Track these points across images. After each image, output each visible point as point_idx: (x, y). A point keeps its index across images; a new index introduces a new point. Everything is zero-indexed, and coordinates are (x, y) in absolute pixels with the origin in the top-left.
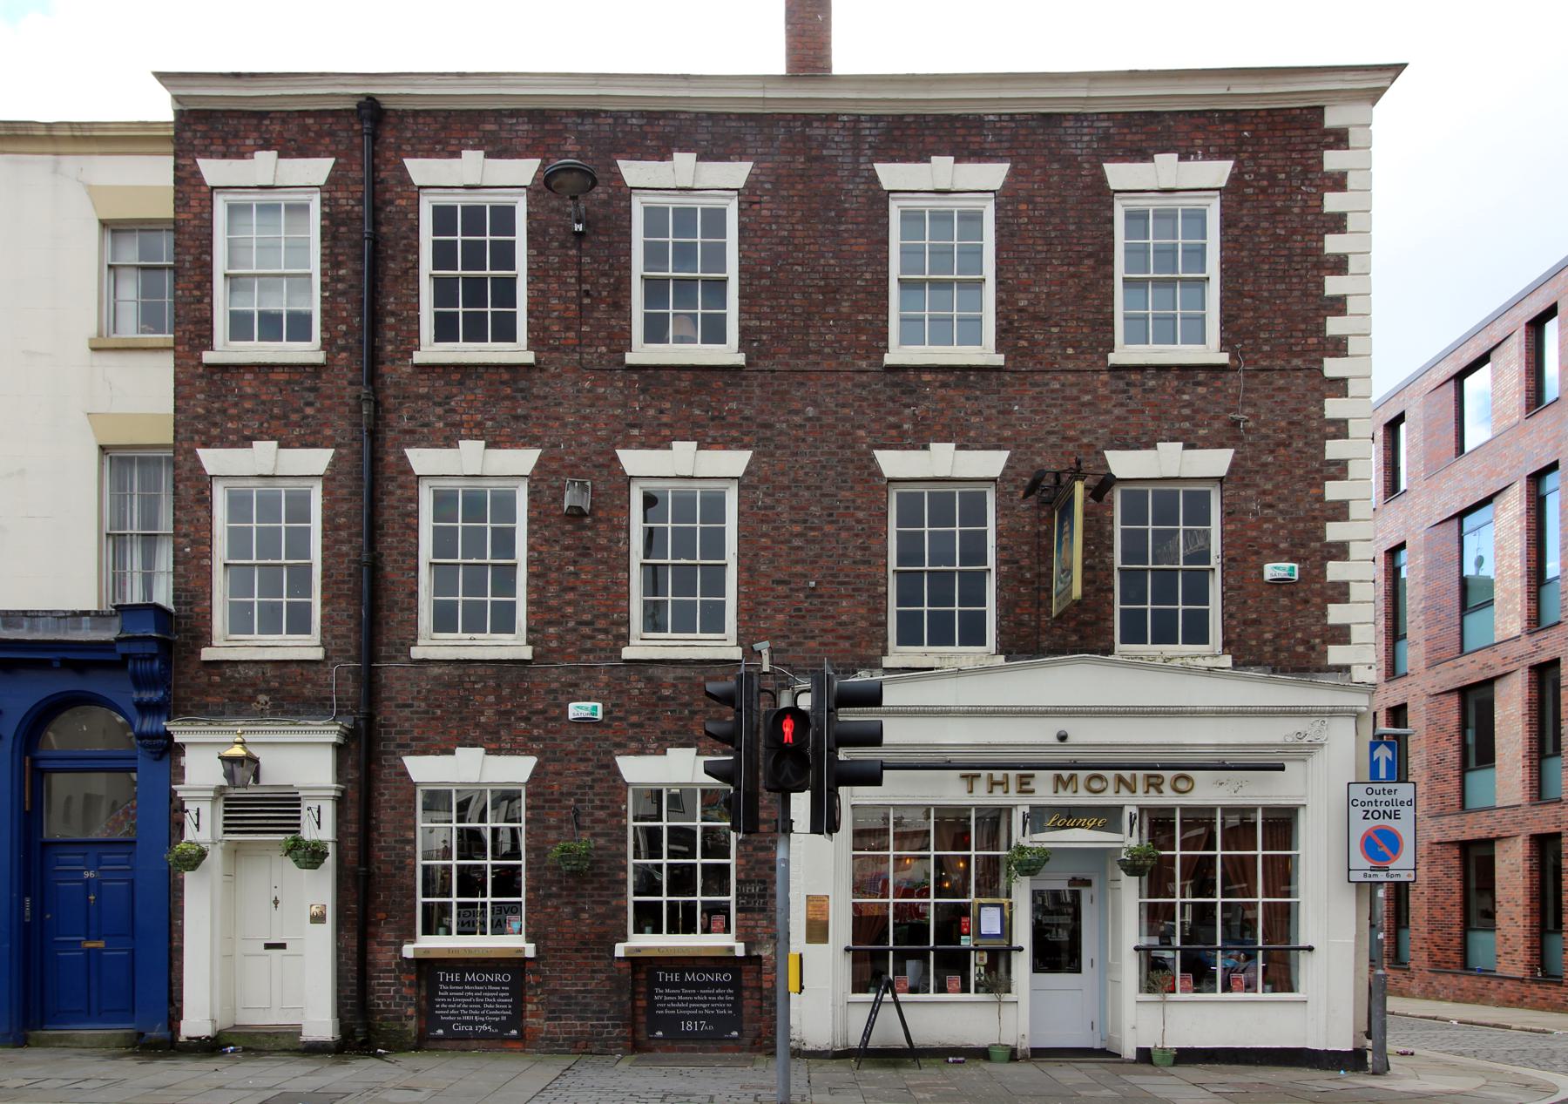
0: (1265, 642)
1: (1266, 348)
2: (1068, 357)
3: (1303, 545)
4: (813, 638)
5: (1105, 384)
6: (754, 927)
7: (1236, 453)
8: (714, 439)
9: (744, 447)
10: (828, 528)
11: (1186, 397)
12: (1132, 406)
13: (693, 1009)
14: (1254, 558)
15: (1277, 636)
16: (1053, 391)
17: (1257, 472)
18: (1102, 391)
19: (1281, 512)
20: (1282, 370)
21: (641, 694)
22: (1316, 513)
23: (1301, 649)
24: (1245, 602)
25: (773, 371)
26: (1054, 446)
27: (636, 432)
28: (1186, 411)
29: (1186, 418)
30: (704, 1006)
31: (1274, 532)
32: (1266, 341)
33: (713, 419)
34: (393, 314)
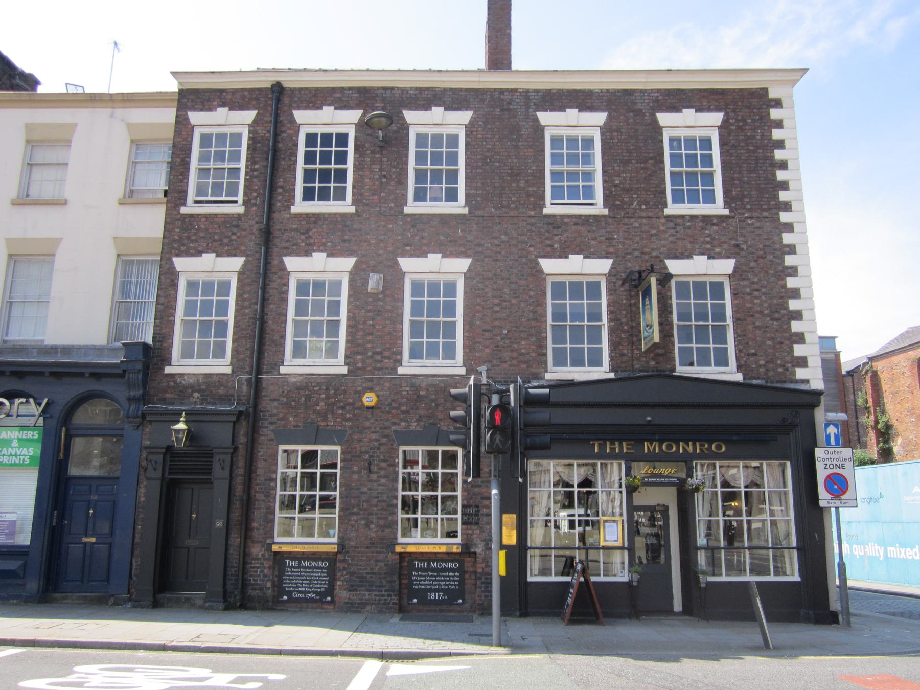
0: (760, 366)
1: (748, 207)
2: (642, 210)
3: (777, 312)
4: (506, 362)
5: (663, 225)
6: (471, 535)
7: (737, 261)
8: (451, 252)
9: (467, 256)
10: (514, 301)
11: (707, 232)
12: (678, 236)
13: (435, 585)
14: (751, 318)
15: (767, 362)
16: (635, 228)
17: (749, 272)
18: (662, 228)
19: (764, 294)
20: (758, 218)
21: (408, 394)
22: (783, 294)
23: (780, 370)
24: (748, 343)
25: (483, 216)
26: (637, 257)
27: (408, 248)
28: (708, 239)
29: (708, 243)
30: (442, 583)
31: (761, 305)
32: (748, 203)
33: (450, 241)
34: (281, 187)
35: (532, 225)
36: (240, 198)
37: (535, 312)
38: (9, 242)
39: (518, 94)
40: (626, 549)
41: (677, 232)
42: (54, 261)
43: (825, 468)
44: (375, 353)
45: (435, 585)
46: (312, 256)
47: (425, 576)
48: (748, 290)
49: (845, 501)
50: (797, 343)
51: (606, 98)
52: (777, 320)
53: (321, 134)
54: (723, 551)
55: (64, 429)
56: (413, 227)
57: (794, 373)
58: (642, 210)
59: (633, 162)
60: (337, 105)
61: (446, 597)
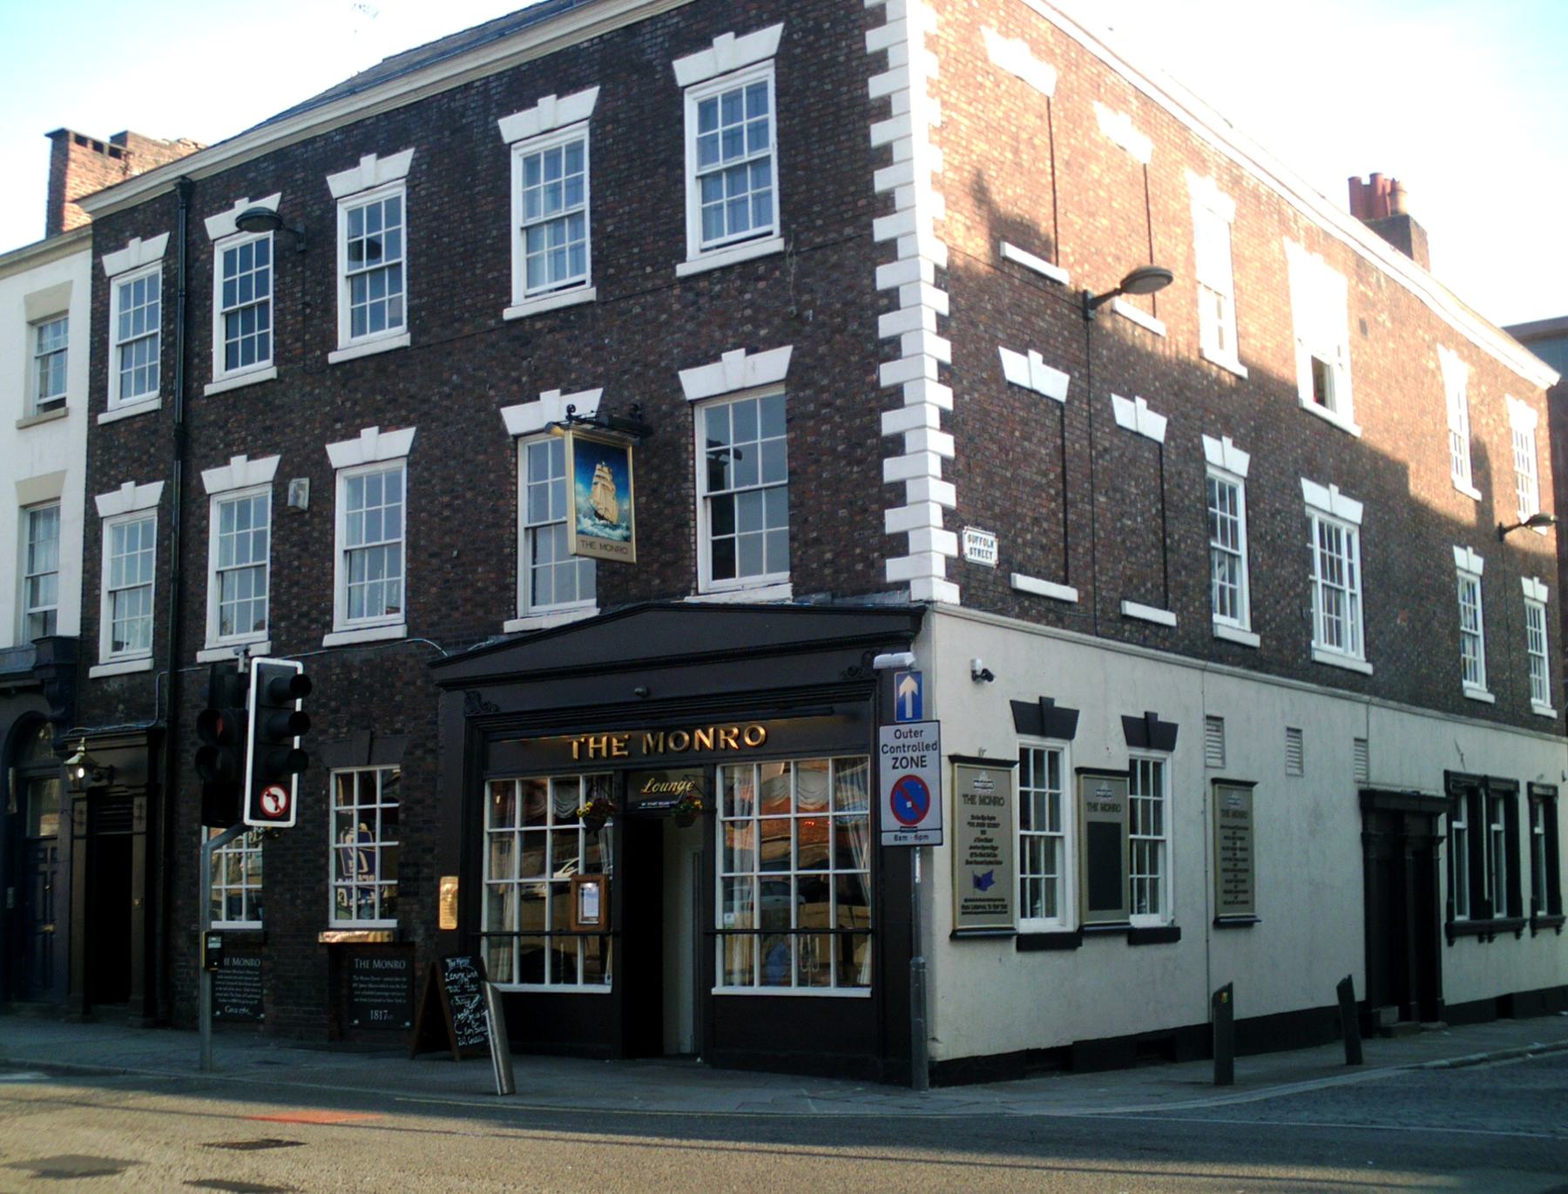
0: (825, 564)
1: (819, 222)
2: (646, 277)
3: (860, 445)
4: (457, 609)
5: (679, 298)
7: (794, 349)
8: (390, 421)
9: (409, 425)
10: (469, 495)
11: (748, 296)
12: (702, 316)
14: (813, 468)
15: (837, 555)
16: (637, 316)
17: (814, 368)
18: (676, 307)
19: (838, 410)
20: (835, 243)
21: (338, 679)
22: (873, 404)
23: (860, 567)
24: (806, 520)
25: (429, 346)
26: (639, 375)
27: (338, 426)
28: (748, 312)
29: (748, 320)
30: (387, 994)
31: (832, 434)
32: (819, 214)
33: (389, 402)
34: (198, 355)
35: (493, 346)
36: (775, 226)
37: (494, 511)
38: (20, 485)
39: (473, 92)
40: (720, 932)
41: (699, 309)
42: (58, 509)
43: (894, 767)
44: (301, 615)
45: (379, 997)
46: (538, 398)
47: (367, 982)
48: (812, 407)
49: (923, 833)
50: (892, 505)
51: (597, 56)
52: (860, 462)
53: (546, 153)
54: (547, 928)
55: (11, 771)
56: (344, 386)
57: (882, 571)
58: (646, 277)
59: (635, 178)
60: (251, 194)
61: (391, 1017)
